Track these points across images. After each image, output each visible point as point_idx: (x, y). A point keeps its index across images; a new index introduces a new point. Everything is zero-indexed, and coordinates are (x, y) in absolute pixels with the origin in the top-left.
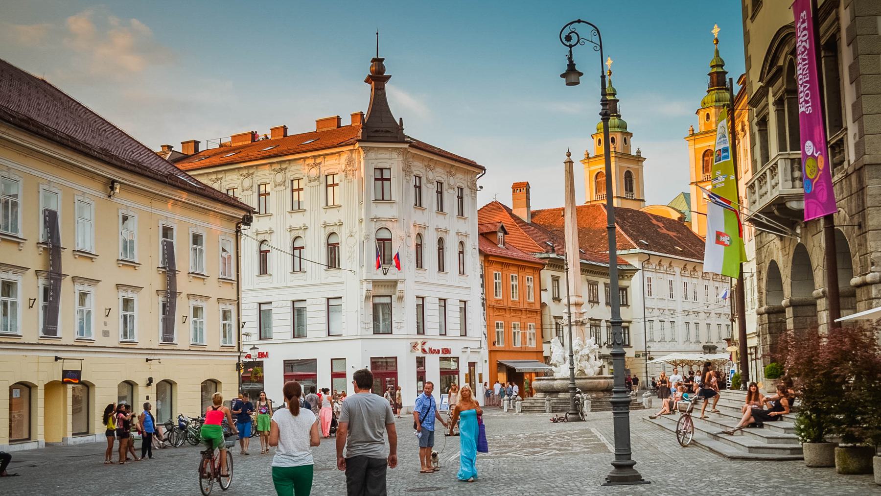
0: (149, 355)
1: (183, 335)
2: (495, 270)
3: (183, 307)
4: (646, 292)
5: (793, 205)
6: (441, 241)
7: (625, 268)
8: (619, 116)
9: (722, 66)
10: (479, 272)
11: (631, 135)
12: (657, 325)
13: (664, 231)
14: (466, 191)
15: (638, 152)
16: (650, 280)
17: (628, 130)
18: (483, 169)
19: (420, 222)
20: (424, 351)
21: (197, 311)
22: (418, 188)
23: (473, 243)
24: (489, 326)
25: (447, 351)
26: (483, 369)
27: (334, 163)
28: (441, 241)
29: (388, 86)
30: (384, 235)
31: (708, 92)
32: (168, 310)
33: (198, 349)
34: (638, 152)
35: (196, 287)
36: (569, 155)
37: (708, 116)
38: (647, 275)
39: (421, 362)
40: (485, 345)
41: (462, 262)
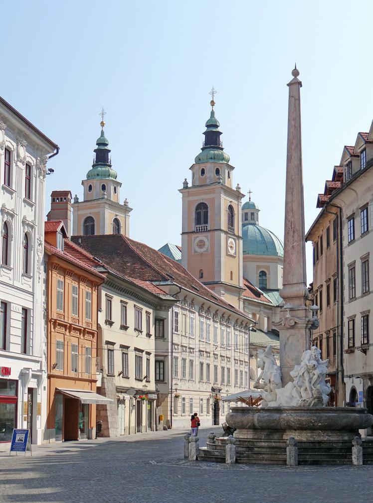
2: (56, 277)
4: (174, 328)
7: (164, 298)
8: (110, 166)
9: (217, 126)
10: (43, 275)
11: (120, 184)
13: (176, 271)
15: (126, 202)
16: (177, 314)
17: (118, 180)
23: (39, 235)
24: (49, 344)
26: (43, 398)
31: (203, 149)
34: (126, 202)
36: (296, 73)
37: (203, 172)
38: (176, 310)
40: (44, 368)
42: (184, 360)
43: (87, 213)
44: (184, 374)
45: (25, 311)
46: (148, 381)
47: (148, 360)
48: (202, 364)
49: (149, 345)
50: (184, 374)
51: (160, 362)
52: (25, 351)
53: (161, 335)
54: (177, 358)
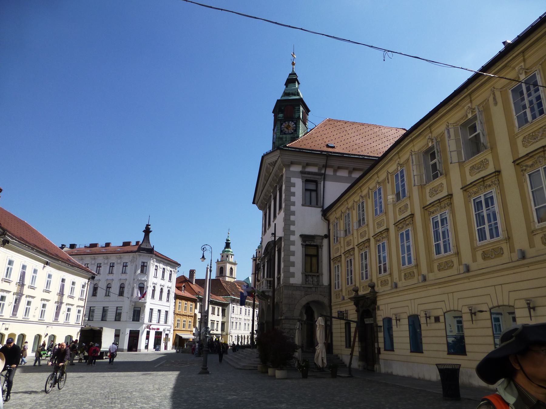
0: (48, 324)
1: (62, 318)
3: (64, 308)
5: (267, 294)
6: (162, 289)
12: (234, 324)
14: (173, 272)
16: (234, 307)
18: (179, 265)
19: (155, 282)
20: (150, 329)
21: (69, 310)
22: (156, 270)
24: (174, 321)
25: (158, 329)
26: (171, 337)
27: (127, 258)
28: (162, 289)
29: (150, 234)
30: (142, 286)
32: (58, 309)
33: (67, 324)
35: (70, 301)
38: (233, 305)
39: (148, 333)
41: (168, 297)
42: (236, 323)
43: (221, 265)
44: (236, 328)
45: (167, 312)
46: (217, 330)
47: (217, 324)
48: (245, 324)
49: (220, 319)
50: (236, 328)
51: (223, 324)
52: (166, 322)
53: (223, 315)
54: (233, 322)
